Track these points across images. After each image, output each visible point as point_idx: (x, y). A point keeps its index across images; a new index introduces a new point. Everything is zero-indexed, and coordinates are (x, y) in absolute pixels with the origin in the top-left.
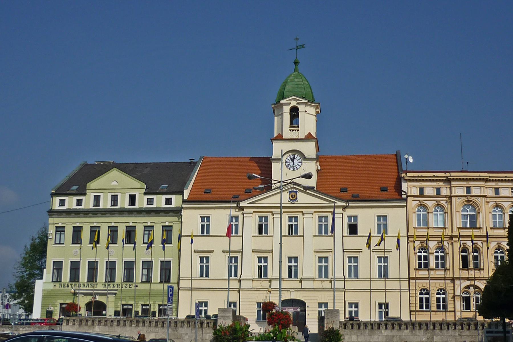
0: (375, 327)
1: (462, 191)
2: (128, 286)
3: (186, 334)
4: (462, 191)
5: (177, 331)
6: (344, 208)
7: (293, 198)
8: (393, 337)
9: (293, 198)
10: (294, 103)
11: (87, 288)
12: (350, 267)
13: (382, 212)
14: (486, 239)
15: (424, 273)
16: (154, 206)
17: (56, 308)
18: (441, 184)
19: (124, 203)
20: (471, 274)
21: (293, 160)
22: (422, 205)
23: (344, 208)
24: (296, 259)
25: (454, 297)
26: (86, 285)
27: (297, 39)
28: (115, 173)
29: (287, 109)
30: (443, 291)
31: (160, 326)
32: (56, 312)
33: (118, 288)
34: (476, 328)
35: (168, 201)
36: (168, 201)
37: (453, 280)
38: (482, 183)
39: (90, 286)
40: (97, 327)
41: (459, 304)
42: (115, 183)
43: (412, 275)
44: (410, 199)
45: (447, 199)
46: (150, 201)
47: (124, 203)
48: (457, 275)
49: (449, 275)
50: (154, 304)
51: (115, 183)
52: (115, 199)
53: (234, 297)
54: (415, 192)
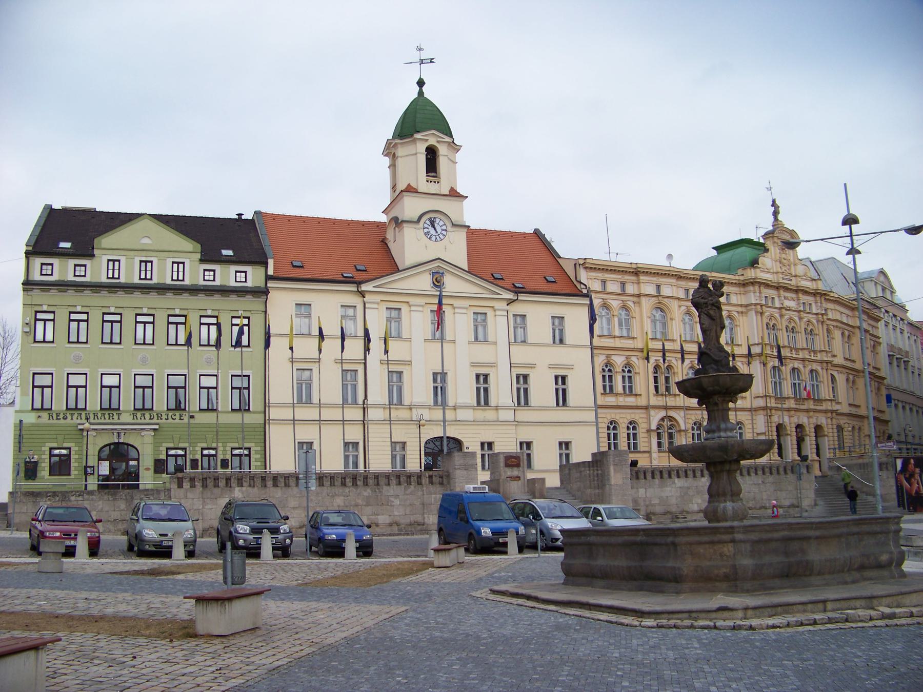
0: (665, 475)
1: (651, 290)
2: (178, 417)
3: (397, 496)
4: (651, 290)
5: (380, 492)
7: (438, 283)
8: (688, 488)
9: (438, 283)
10: (432, 141)
11: (103, 421)
12: (518, 389)
13: (558, 311)
14: (679, 355)
15: (611, 400)
17: (43, 457)
18: (627, 278)
21: (432, 224)
23: (510, 302)
24: (444, 375)
25: (649, 431)
26: (99, 416)
29: (422, 148)
30: (633, 425)
31: (350, 484)
32: (43, 465)
33: (159, 421)
34: (778, 473)
37: (647, 408)
38: (673, 281)
39: (107, 416)
40: (237, 489)
42: (146, 241)
43: (599, 403)
45: (635, 299)
47: (162, 274)
48: (652, 403)
49: (642, 402)
50: (225, 447)
51: (146, 241)
53: (354, 434)
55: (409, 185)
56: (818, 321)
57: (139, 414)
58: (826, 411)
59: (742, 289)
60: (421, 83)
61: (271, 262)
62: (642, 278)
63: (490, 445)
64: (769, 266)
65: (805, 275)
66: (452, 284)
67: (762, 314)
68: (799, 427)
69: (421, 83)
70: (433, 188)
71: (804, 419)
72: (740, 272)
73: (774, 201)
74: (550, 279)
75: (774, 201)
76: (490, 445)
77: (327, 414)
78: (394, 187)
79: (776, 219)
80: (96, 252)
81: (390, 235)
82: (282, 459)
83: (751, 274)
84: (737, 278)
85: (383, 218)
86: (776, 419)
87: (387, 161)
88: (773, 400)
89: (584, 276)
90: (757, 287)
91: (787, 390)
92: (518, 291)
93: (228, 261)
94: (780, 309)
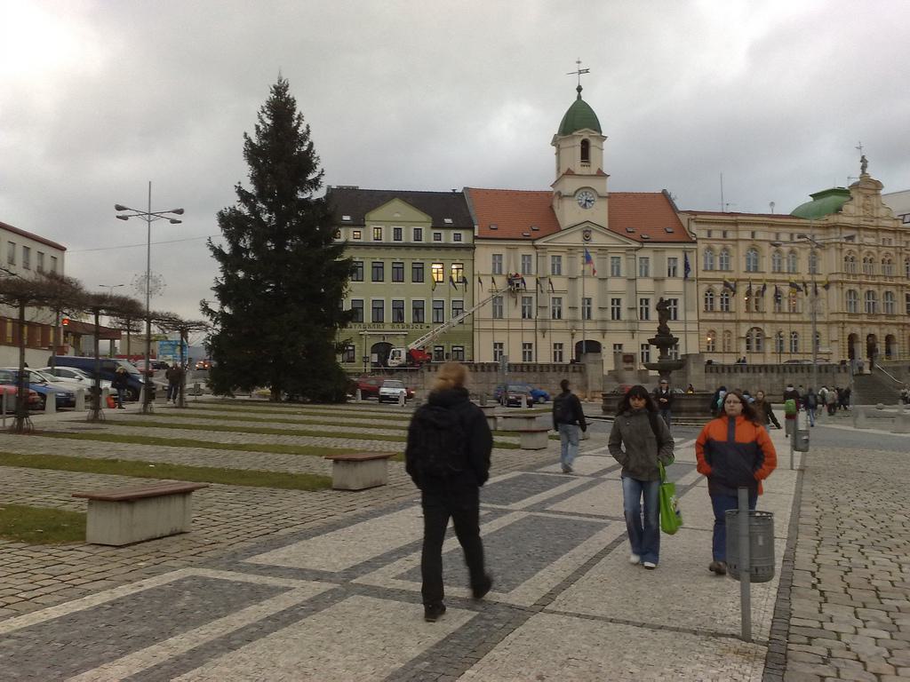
0: (732, 370)
4: (747, 235)
6: (637, 249)
7: (587, 238)
9: (587, 238)
10: (586, 136)
15: (711, 316)
16: (442, 242)
18: (727, 228)
19: (408, 237)
20: (756, 317)
22: (710, 249)
23: (637, 249)
27: (579, 62)
28: (397, 204)
29: (578, 142)
35: (457, 237)
36: (457, 237)
38: (766, 228)
41: (743, 345)
42: (397, 215)
43: (701, 318)
44: (699, 241)
45: (735, 243)
46: (438, 236)
47: (408, 237)
51: (397, 215)
52: (398, 232)
53: (529, 338)
54: (703, 234)
55: (569, 169)
56: (896, 253)
57: (395, 325)
58: (898, 324)
59: (825, 231)
60: (579, 89)
61: (476, 227)
62: (740, 227)
63: (620, 346)
64: (852, 212)
65: (888, 216)
66: (598, 239)
67: (841, 250)
68: (871, 336)
69: (579, 89)
70: (585, 171)
71: (875, 330)
72: (826, 217)
73: (863, 157)
74: (669, 230)
75: (863, 157)
76: (620, 346)
77: (513, 325)
78: (558, 169)
79: (863, 172)
80: (366, 223)
81: (555, 204)
82: (485, 355)
83: (833, 219)
84: (822, 222)
85: (551, 189)
86: (848, 330)
87: (554, 149)
88: (846, 316)
89: (694, 228)
90: (838, 230)
91: (861, 308)
92: (643, 241)
93: (449, 227)
94: (859, 245)
